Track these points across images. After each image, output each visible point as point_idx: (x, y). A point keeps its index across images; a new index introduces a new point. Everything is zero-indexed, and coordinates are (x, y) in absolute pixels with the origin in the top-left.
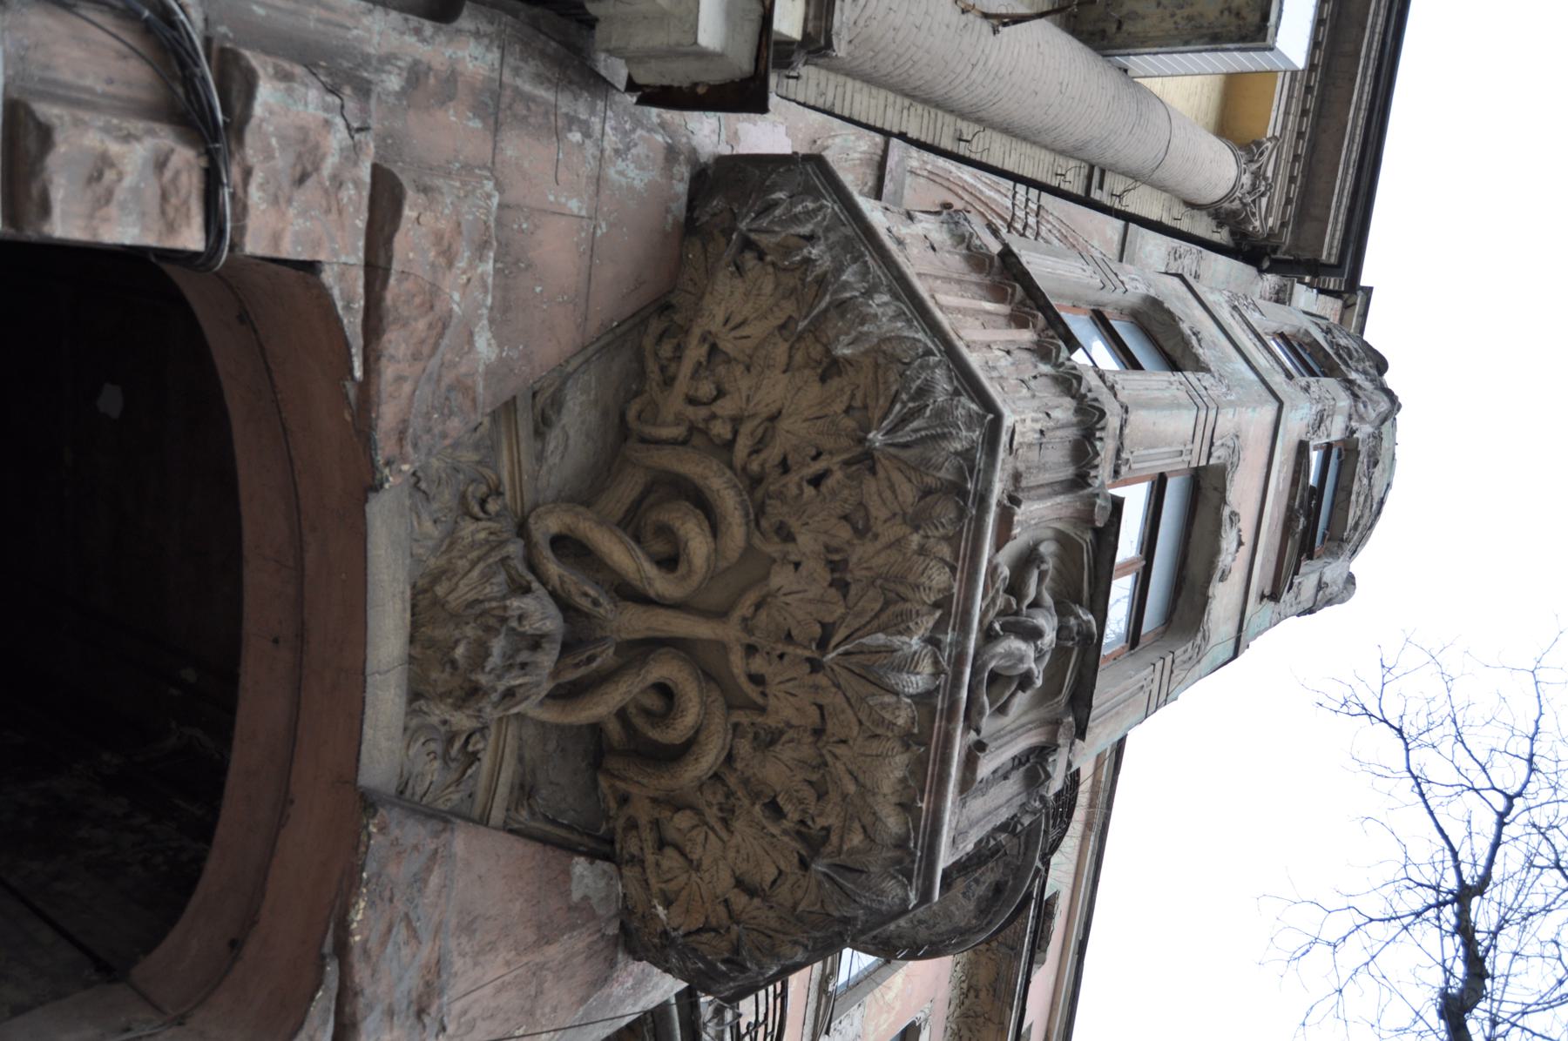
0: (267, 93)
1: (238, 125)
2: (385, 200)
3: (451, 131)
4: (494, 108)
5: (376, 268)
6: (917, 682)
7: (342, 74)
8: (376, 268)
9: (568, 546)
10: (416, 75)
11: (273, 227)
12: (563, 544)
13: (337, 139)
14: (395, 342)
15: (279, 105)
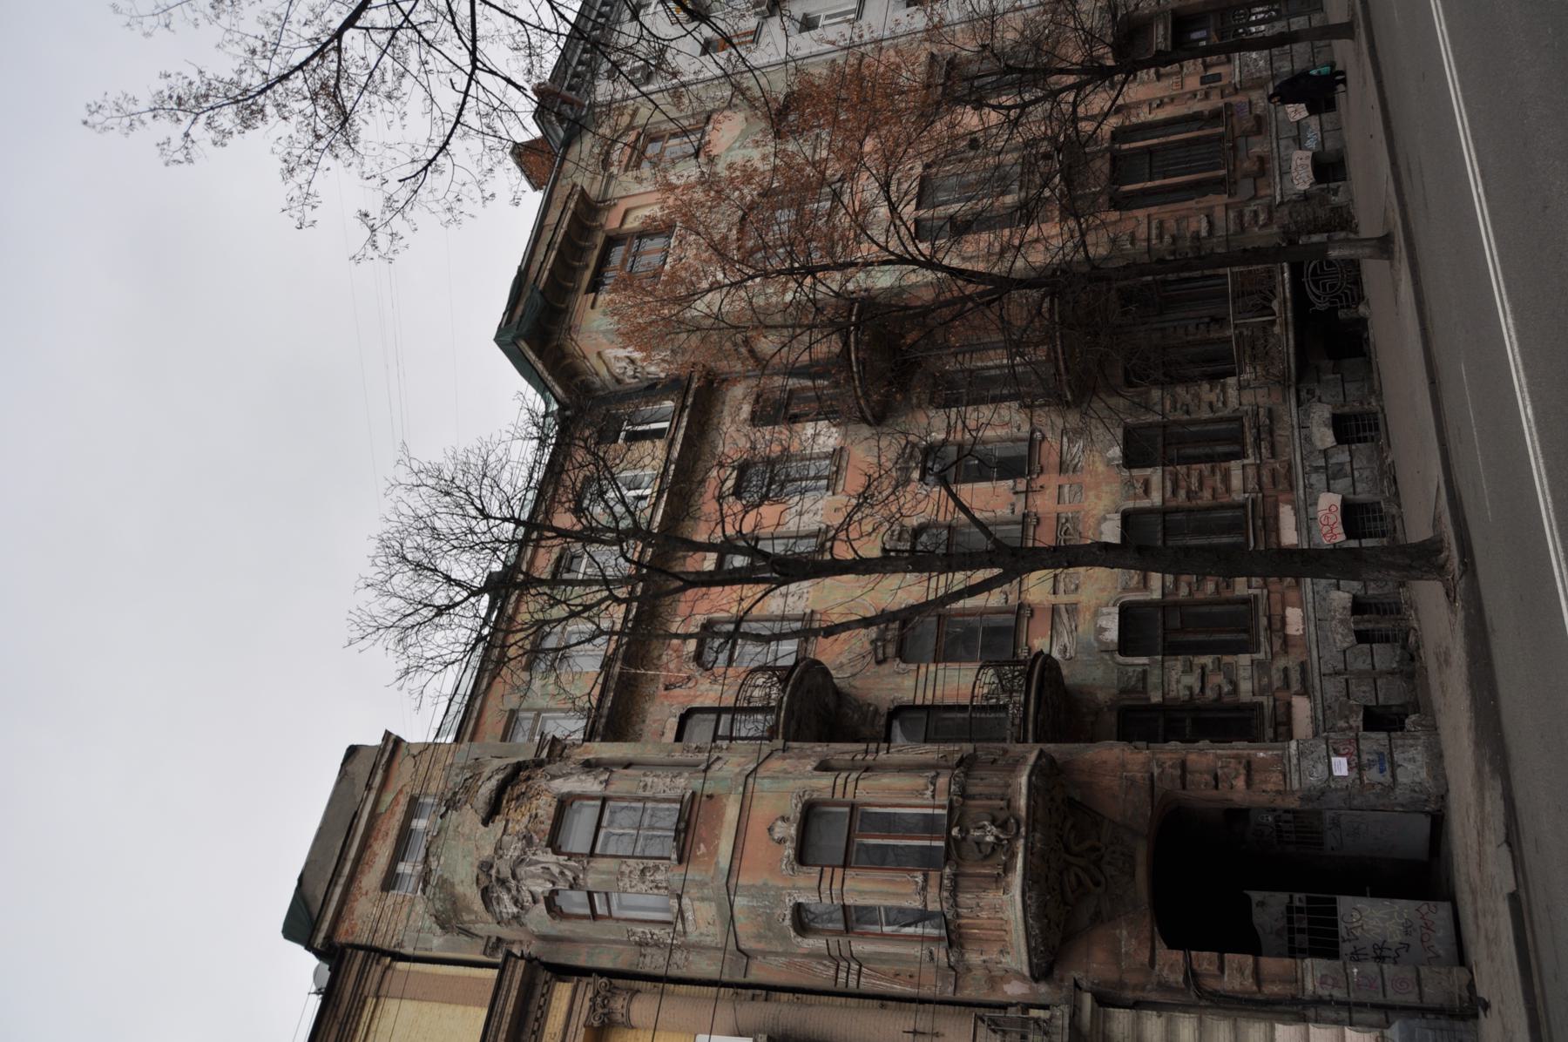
0: (1181, 979)
1: (1186, 974)
2: (1152, 962)
3: (1131, 979)
4: (1122, 985)
5: (1153, 949)
6: (1038, 835)
7: (1163, 986)
8: (1153, 949)
9: (1097, 884)
10: (1143, 989)
11: (1178, 956)
12: (1097, 884)
13: (1165, 973)
14: (1148, 934)
15: (1178, 978)
